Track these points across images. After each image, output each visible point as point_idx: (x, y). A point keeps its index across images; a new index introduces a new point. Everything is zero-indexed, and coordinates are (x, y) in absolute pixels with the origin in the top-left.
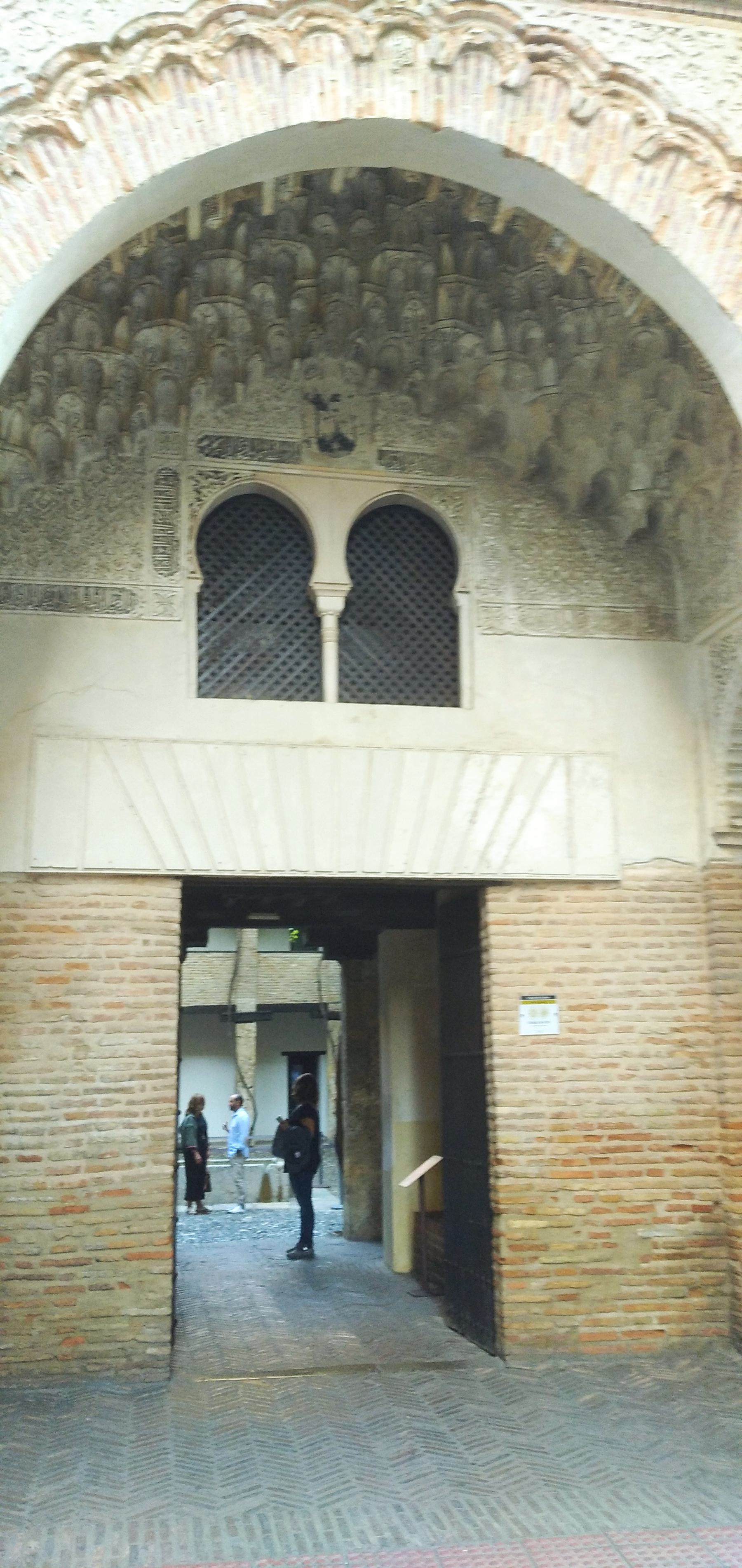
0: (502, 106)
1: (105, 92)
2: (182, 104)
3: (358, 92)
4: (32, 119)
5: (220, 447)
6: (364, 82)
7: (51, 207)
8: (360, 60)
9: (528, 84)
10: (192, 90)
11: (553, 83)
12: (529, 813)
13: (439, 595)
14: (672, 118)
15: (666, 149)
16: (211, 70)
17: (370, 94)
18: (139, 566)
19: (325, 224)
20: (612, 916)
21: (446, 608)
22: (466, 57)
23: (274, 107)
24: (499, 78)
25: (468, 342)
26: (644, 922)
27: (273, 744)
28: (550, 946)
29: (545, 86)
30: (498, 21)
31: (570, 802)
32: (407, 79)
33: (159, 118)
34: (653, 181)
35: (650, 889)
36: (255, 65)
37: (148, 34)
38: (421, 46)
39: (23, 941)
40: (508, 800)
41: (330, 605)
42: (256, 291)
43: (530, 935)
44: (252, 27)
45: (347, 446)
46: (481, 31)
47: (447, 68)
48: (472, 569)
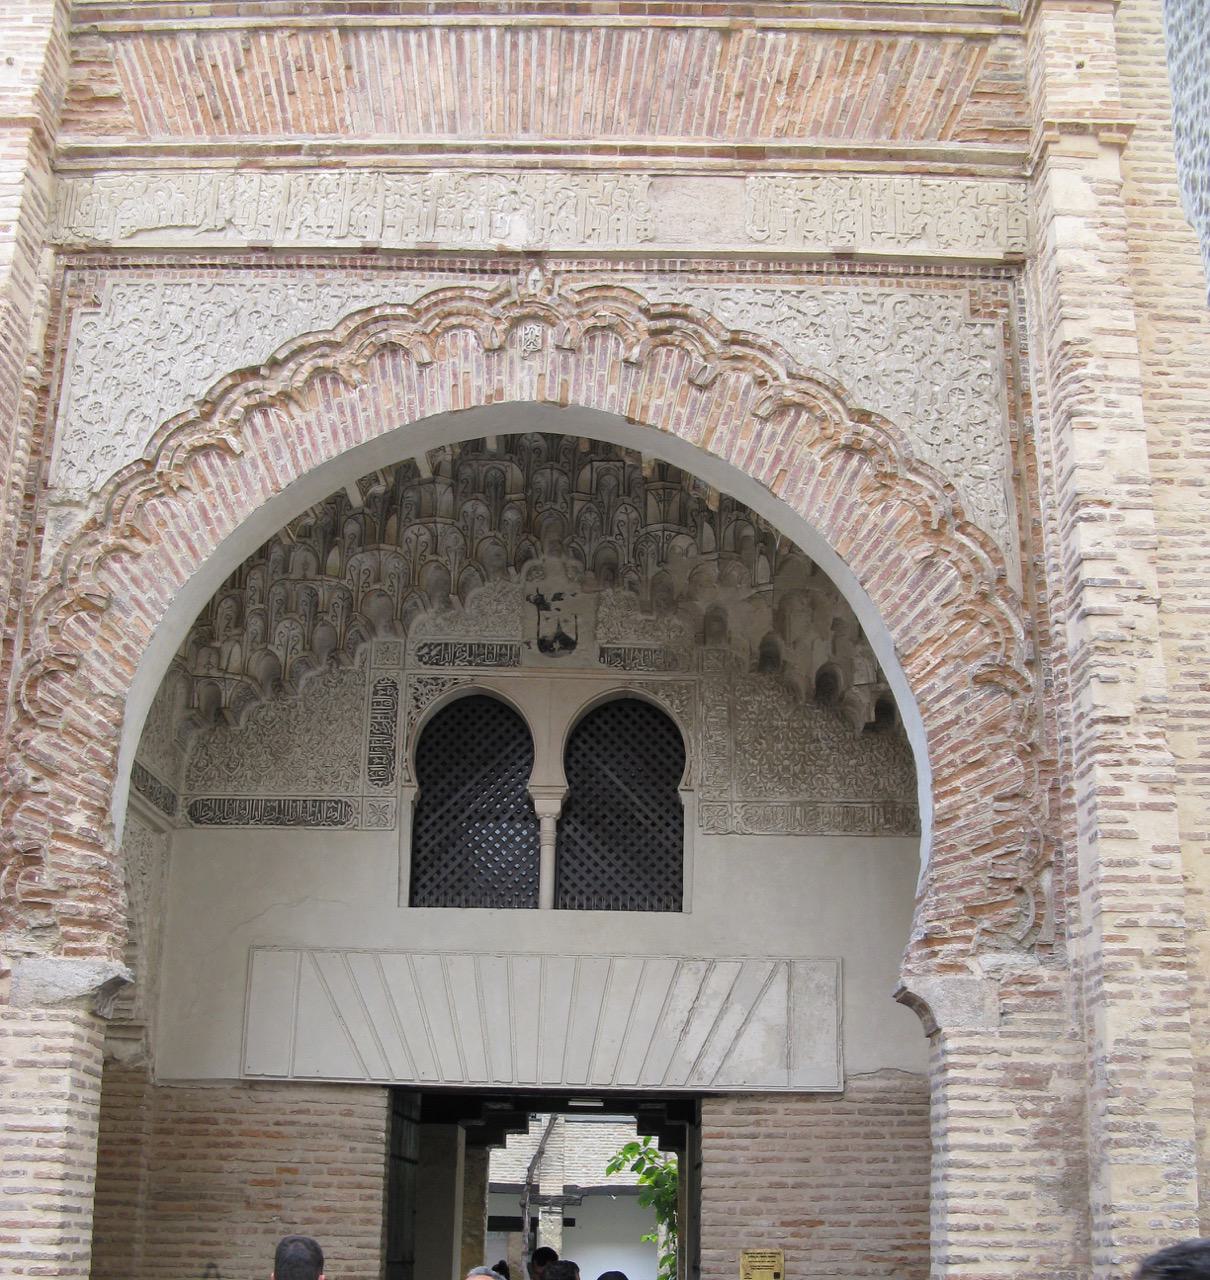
1: (262, 407)
3: (490, 380)
4: (198, 438)
6: (495, 371)
7: (211, 515)
9: (652, 356)
10: (337, 394)
13: (668, 790)
14: (790, 375)
15: (783, 408)
16: (356, 376)
21: (675, 804)
22: (593, 338)
23: (411, 402)
24: (623, 354)
32: (535, 363)
33: (308, 424)
34: (773, 435)
36: (395, 367)
37: (302, 350)
38: (550, 332)
44: (394, 334)
46: (605, 311)
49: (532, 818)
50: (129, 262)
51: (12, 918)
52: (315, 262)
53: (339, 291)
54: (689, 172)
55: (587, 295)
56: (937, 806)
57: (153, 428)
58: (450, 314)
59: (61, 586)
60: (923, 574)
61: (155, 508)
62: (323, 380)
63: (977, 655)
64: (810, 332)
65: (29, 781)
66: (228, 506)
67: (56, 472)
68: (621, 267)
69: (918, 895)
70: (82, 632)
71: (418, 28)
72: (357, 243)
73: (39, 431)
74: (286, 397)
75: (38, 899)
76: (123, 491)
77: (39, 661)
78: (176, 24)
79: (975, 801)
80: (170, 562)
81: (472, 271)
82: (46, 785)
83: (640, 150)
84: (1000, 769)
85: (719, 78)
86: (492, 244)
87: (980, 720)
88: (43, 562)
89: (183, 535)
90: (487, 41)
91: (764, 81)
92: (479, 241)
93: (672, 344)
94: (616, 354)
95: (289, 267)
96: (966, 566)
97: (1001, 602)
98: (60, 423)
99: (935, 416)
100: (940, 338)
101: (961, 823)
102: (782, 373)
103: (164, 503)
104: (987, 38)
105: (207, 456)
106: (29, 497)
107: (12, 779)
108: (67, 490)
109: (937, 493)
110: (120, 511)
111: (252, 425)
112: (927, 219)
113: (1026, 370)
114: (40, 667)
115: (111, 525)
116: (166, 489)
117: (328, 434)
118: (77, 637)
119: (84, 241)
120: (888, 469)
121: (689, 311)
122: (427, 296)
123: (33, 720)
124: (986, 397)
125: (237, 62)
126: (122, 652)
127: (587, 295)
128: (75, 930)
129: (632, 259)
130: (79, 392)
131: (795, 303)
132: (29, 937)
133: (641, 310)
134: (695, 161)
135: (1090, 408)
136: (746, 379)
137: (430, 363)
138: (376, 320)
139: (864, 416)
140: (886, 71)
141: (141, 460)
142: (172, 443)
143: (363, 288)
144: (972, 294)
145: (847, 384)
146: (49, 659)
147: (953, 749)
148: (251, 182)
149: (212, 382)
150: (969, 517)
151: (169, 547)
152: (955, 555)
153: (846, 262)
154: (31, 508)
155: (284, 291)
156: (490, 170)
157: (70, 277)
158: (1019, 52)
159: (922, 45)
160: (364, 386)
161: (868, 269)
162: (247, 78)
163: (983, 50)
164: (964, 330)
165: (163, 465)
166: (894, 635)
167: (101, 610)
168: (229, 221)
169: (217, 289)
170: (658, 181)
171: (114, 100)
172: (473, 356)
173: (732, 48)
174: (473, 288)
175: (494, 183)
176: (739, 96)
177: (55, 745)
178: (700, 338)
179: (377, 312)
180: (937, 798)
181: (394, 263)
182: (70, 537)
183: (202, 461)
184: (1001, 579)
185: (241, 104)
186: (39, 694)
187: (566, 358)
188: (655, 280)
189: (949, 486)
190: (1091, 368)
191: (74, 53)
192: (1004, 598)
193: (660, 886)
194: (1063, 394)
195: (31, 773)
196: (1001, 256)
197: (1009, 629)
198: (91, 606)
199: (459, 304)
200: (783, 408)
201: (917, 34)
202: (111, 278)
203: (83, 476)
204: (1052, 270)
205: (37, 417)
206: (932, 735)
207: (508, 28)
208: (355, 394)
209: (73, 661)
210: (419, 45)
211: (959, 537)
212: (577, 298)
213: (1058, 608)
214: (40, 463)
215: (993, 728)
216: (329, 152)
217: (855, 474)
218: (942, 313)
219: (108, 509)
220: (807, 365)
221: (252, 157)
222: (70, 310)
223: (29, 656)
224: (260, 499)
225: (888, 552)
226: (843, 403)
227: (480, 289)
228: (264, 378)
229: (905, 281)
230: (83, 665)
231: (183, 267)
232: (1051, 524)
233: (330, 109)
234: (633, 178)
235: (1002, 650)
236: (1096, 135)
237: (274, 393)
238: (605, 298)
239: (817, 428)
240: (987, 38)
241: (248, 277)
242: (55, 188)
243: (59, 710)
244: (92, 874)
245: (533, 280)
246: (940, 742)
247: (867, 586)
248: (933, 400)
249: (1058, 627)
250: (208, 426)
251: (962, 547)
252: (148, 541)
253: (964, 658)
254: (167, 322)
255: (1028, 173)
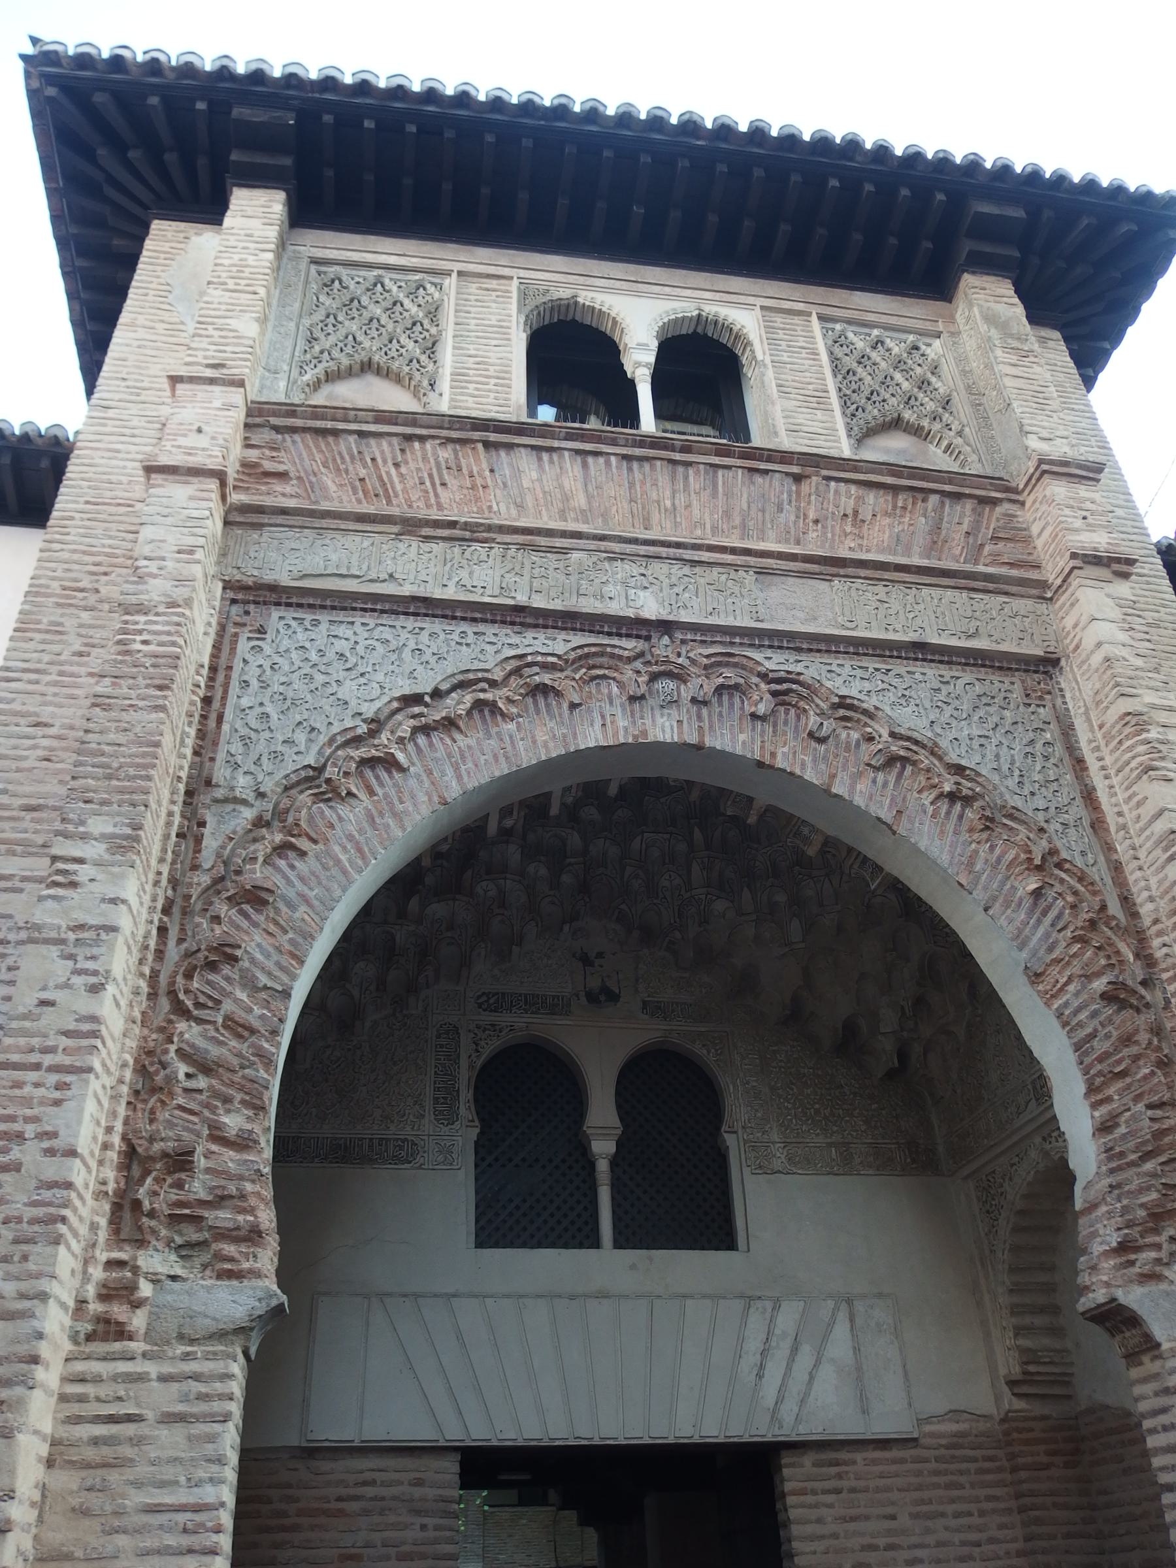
0: (753, 729)
1: (426, 730)
2: (489, 737)
3: (634, 723)
5: (496, 1002)
7: (378, 820)
8: (633, 699)
11: (793, 711)
12: (817, 1364)
14: (893, 735)
16: (514, 710)
17: (643, 724)
18: (423, 1116)
19: (591, 813)
20: (913, 1480)
22: (720, 695)
25: (720, 906)
26: (949, 1486)
27: (552, 1296)
28: (853, 1519)
29: (787, 713)
30: (744, 667)
31: (856, 1350)
32: (674, 712)
33: (469, 747)
35: (947, 1447)
36: (548, 705)
37: (461, 685)
38: (682, 687)
39: (295, 1528)
40: (795, 1350)
41: (603, 1148)
42: (531, 869)
43: (831, 1506)
44: (546, 678)
45: (613, 997)
46: (730, 675)
47: (705, 703)
48: (738, 1109)
49: (591, 1165)
50: (294, 600)
51: (154, 1232)
52: (469, 615)
53: (493, 639)
54: (786, 573)
55: (713, 660)
56: (1097, 1114)
57: (323, 739)
58: (594, 667)
59: (222, 879)
60: (1035, 904)
61: (322, 812)
62: (481, 711)
63: (1098, 974)
64: (903, 701)
65: (181, 1076)
66: (395, 815)
67: (221, 773)
68: (737, 640)
69: (1079, 1205)
70: (245, 924)
71: (550, 450)
72: (512, 602)
73: (201, 734)
74: (450, 724)
75: (187, 1211)
76: (294, 792)
77: (199, 950)
78: (341, 426)
79: (1129, 1110)
80: (338, 862)
81: (609, 634)
82: (202, 1082)
83: (747, 552)
84: (1145, 1078)
85: (798, 508)
86: (630, 613)
87: (1115, 1033)
88: (204, 853)
89: (350, 837)
90: (608, 464)
91: (833, 513)
92: (615, 608)
93: (789, 704)
94: (742, 709)
95: (444, 617)
96: (1070, 899)
97: (1106, 929)
98: (226, 727)
99: (1017, 773)
100: (1007, 713)
101: (1123, 1130)
102: (885, 734)
103: (331, 807)
104: (994, 502)
105: (373, 768)
106: (189, 793)
107: (162, 1073)
108: (232, 789)
109: (1031, 836)
110: (287, 811)
111: (416, 744)
112: (978, 623)
113: (1077, 742)
114: (200, 955)
115: (276, 823)
116: (332, 794)
117: (490, 757)
118: (238, 928)
119: (252, 579)
120: (988, 813)
121: (801, 678)
122: (574, 649)
123: (189, 1011)
124: (1052, 761)
125: (394, 458)
126: (287, 947)
127: (713, 660)
128: (230, 1249)
129: (747, 635)
130: (245, 702)
131: (885, 678)
132: (173, 1257)
133: (759, 675)
134: (792, 565)
135: (1163, 764)
136: (855, 735)
137: (580, 705)
138: (529, 665)
139: (959, 770)
140: (925, 516)
141: (309, 766)
142: (340, 753)
143: (515, 639)
144: (1023, 682)
145: (944, 743)
146: (211, 949)
147: (1100, 1059)
148: (411, 547)
149: (378, 704)
150: (1064, 855)
151: (337, 849)
152: (1058, 887)
153: (920, 651)
154: (191, 804)
155: (442, 636)
156: (622, 557)
157: (235, 609)
158: (1018, 513)
159: (947, 502)
160: (521, 720)
161: (937, 657)
162: (403, 470)
163: (992, 510)
164: (1022, 708)
165: (330, 772)
166: (1024, 955)
167: (265, 903)
168: (391, 576)
169: (381, 628)
170: (761, 577)
171: (282, 476)
172: (617, 702)
173: (805, 487)
174: (614, 646)
175: (627, 567)
176: (816, 522)
177: (213, 1039)
178: (813, 701)
179: (529, 658)
180: (1094, 1106)
181: (541, 621)
182: (234, 832)
183: (368, 773)
184: (1103, 907)
185: (399, 487)
186: (196, 985)
187: (699, 710)
188: (769, 653)
189: (1042, 830)
190: (1153, 734)
191: (246, 438)
192: (1107, 925)
193: (714, 1227)
194: (1130, 755)
195: (182, 1069)
196: (1040, 652)
197: (1118, 952)
198: (256, 898)
199: (604, 660)
200: (892, 760)
201: (942, 493)
202: (276, 613)
203: (249, 777)
204: (1097, 659)
205: (200, 722)
206: (1077, 1047)
207: (625, 457)
208: (511, 726)
209: (238, 953)
210: (551, 462)
211: (1057, 872)
212: (705, 661)
213: (1160, 934)
214: (202, 763)
215: (1127, 1040)
216: (482, 528)
217: (961, 817)
218: (1003, 694)
219: (274, 808)
220: (907, 726)
221: (410, 526)
222: (236, 635)
223: (185, 945)
224: (425, 810)
225: (1003, 883)
226: (940, 759)
227: (621, 647)
228: (427, 705)
229: (968, 668)
230: (246, 957)
231: (344, 609)
232: (1136, 863)
233: (477, 499)
234: (741, 573)
235: (1116, 972)
236: (1108, 566)
237: (438, 718)
238: (727, 664)
239: (922, 778)
240: (994, 502)
241: (410, 623)
242: (225, 535)
243: (218, 1002)
244: (253, 1181)
245: (663, 646)
246: (1086, 1053)
247: (991, 912)
248: (1012, 763)
249: (1165, 950)
250: (376, 742)
251: (1062, 881)
252: (315, 842)
253: (1086, 976)
254: (334, 651)
255: (1049, 595)
